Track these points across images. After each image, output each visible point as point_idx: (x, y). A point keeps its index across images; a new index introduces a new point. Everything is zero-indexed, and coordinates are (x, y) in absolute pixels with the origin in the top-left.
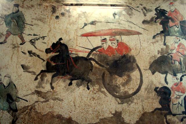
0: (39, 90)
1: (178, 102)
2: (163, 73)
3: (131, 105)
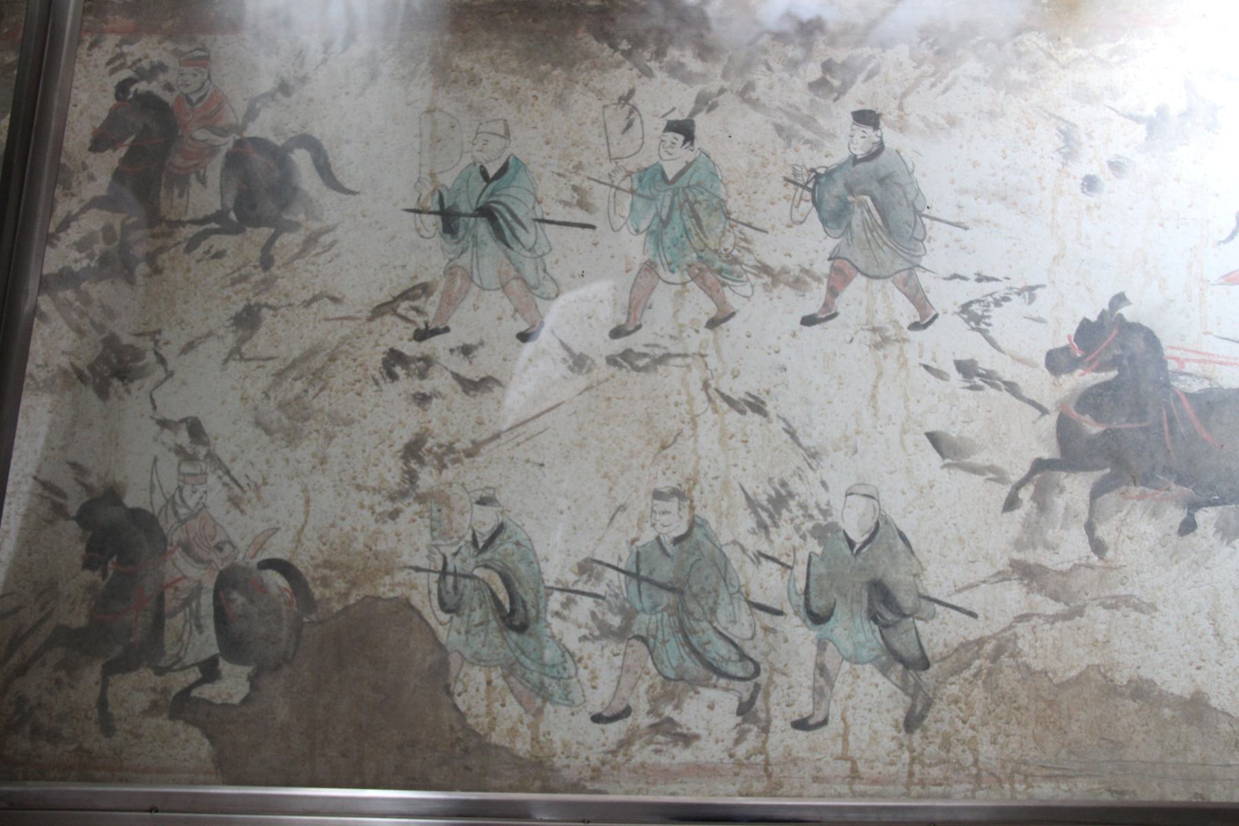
0: (1030, 557)
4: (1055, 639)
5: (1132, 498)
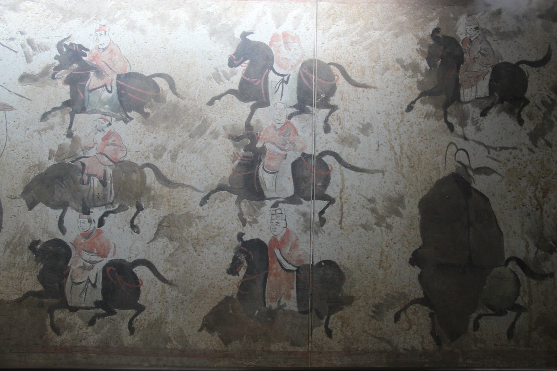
1: (86, 279)
2: (55, 207)
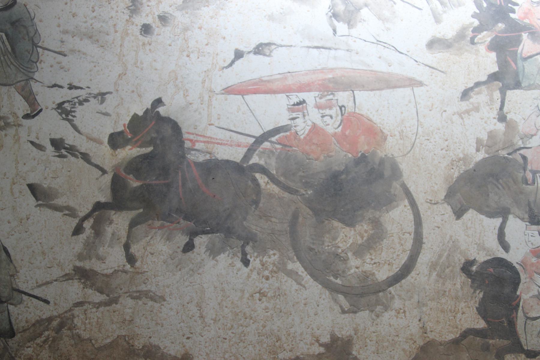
0: (87, 265)
2: (491, 215)
3: (380, 318)
4: (98, 318)
5: (155, 228)
